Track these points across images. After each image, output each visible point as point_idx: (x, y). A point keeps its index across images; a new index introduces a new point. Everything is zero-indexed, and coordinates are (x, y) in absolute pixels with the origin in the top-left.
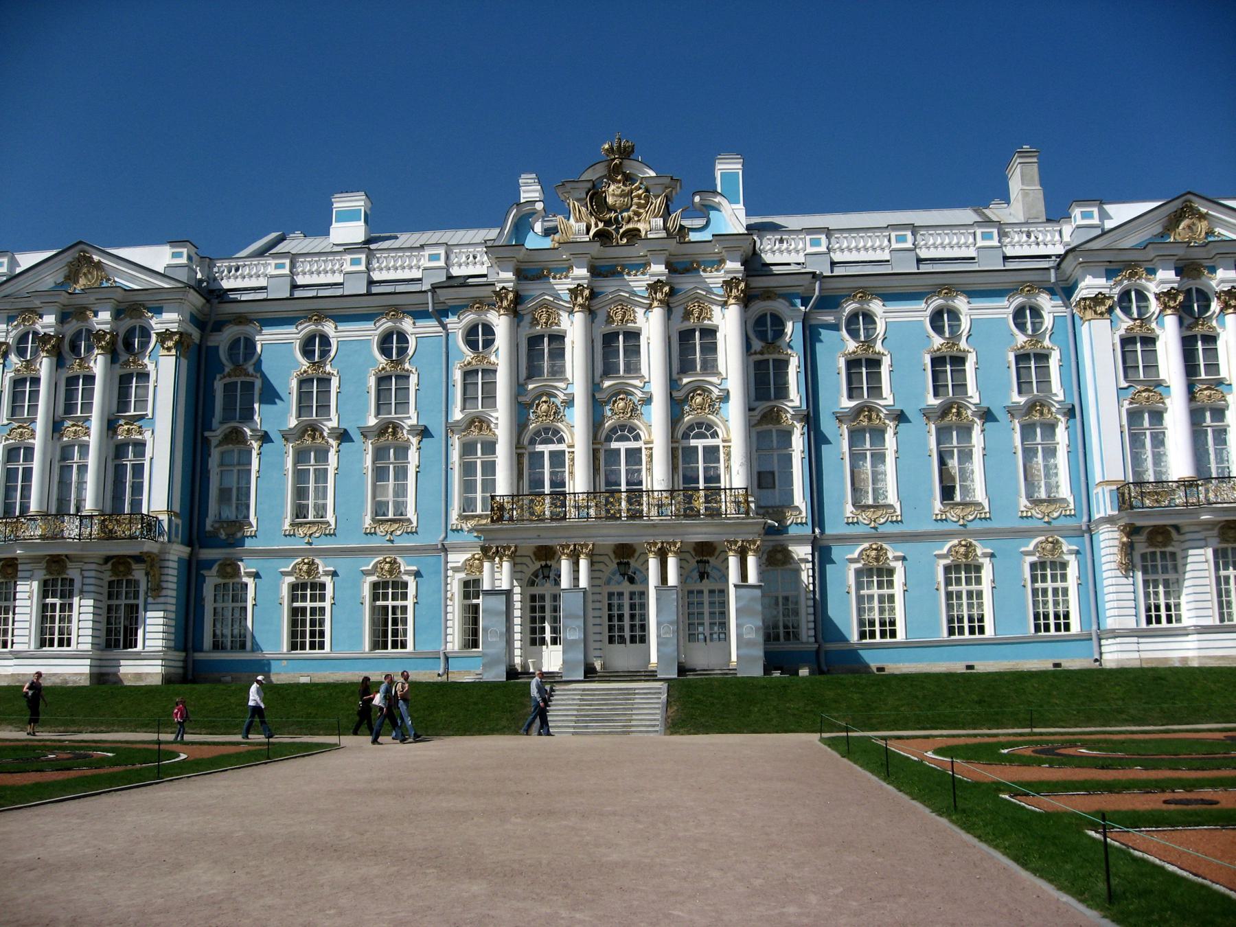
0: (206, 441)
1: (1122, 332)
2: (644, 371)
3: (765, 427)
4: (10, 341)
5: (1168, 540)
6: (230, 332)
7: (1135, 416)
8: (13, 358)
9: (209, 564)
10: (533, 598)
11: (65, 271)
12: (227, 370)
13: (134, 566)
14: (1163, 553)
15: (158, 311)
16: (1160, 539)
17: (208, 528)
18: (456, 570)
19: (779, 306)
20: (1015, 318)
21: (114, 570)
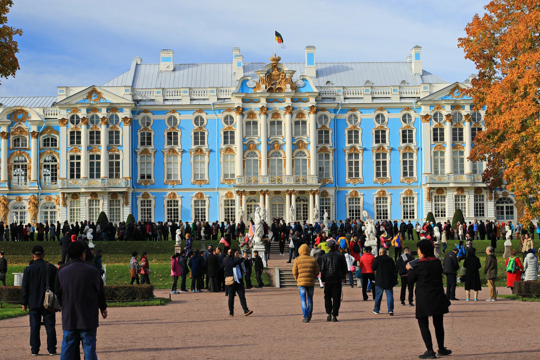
0: (136, 153)
1: (433, 127)
2: (283, 134)
3: (321, 153)
4: (69, 118)
5: (443, 192)
6: (142, 115)
7: (435, 153)
8: (70, 124)
9: (139, 194)
10: (248, 206)
11: (87, 95)
12: (142, 128)
13: (119, 195)
14: (441, 196)
15: (121, 111)
16: (440, 192)
17: (138, 182)
18: (222, 196)
19: (327, 113)
20: (403, 118)
21: (112, 197)
